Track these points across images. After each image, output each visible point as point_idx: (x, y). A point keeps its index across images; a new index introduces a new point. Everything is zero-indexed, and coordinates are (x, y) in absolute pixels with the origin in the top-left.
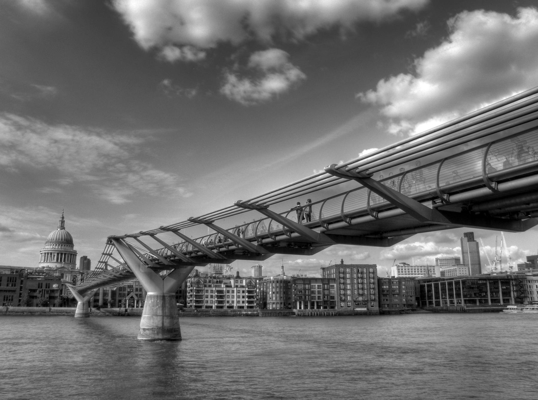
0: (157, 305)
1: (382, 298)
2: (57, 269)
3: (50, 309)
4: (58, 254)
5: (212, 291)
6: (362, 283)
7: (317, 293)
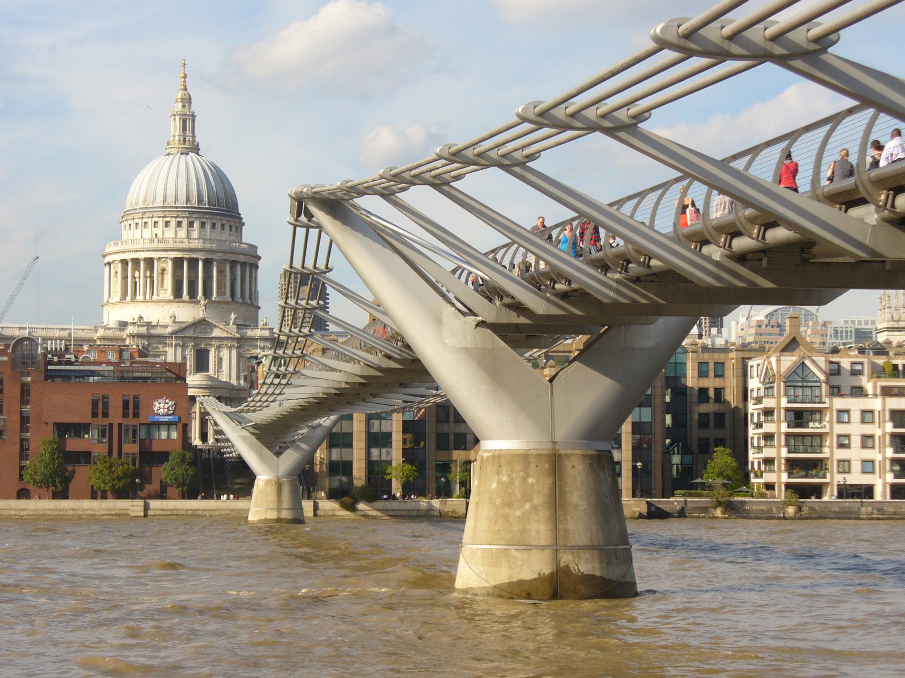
0: (527, 497)
2: (183, 333)
3: (146, 508)
4: (178, 263)
5: (867, 415)
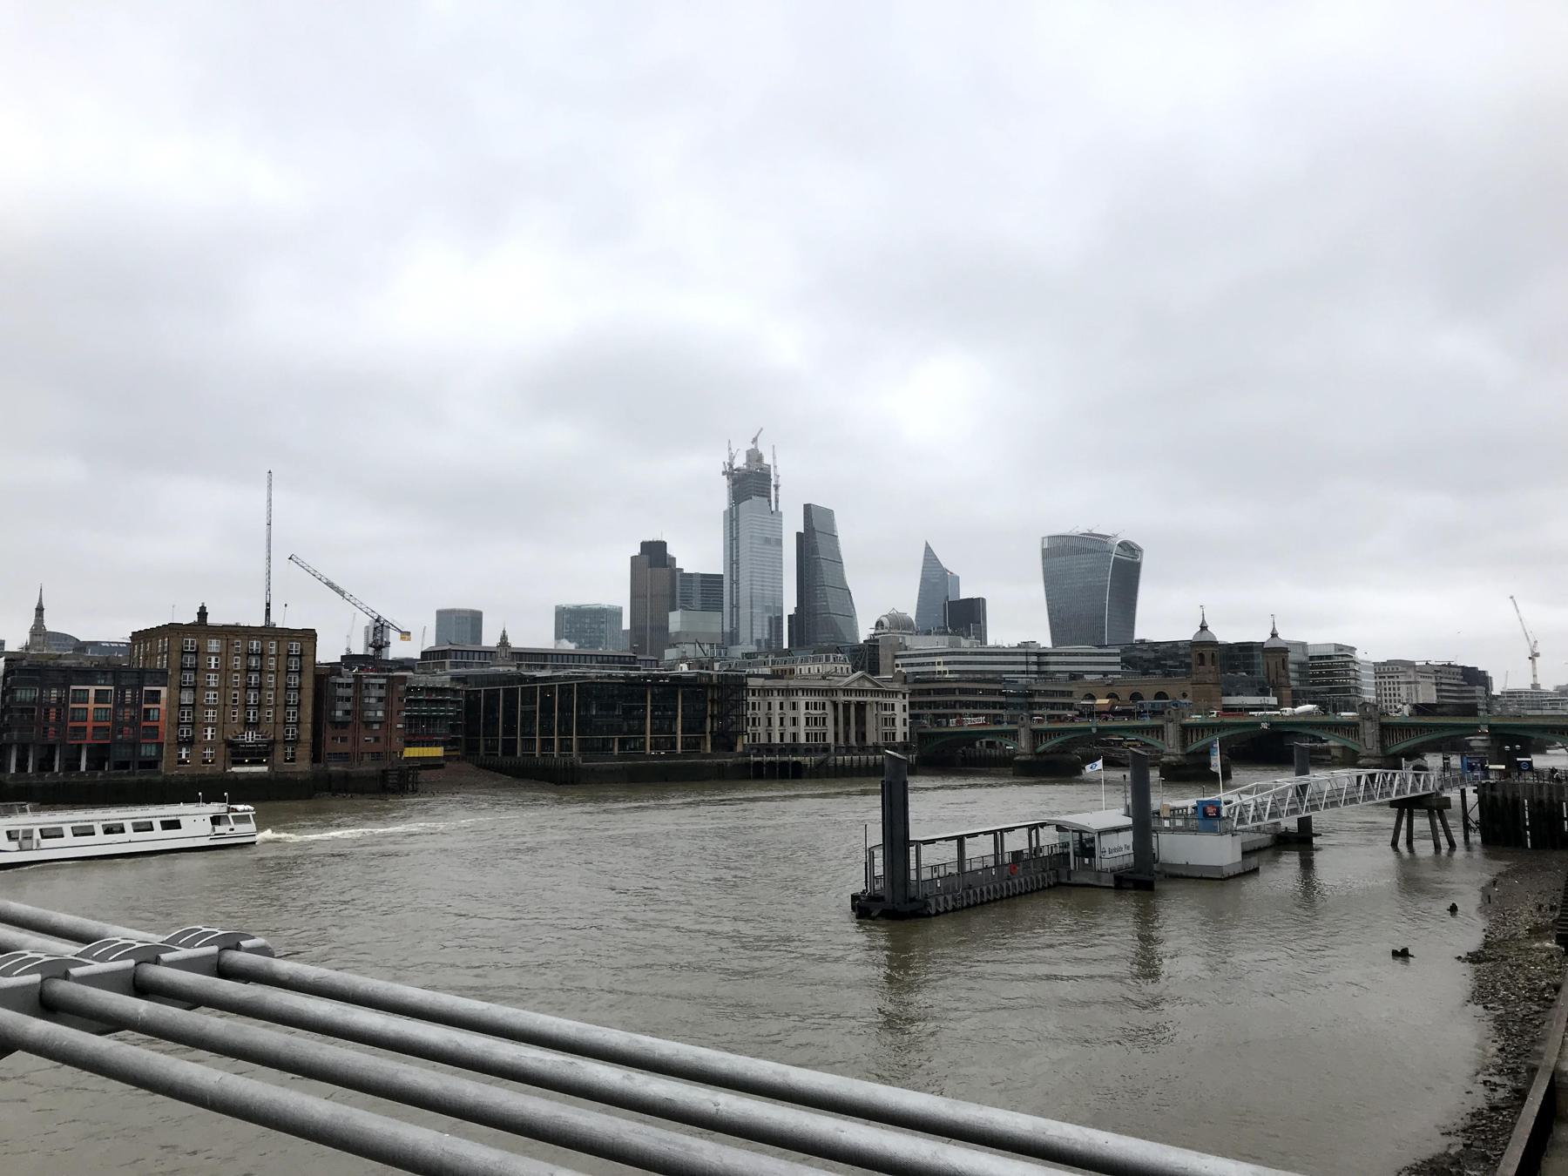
1: (329, 733)
6: (259, 688)
7: (90, 718)
